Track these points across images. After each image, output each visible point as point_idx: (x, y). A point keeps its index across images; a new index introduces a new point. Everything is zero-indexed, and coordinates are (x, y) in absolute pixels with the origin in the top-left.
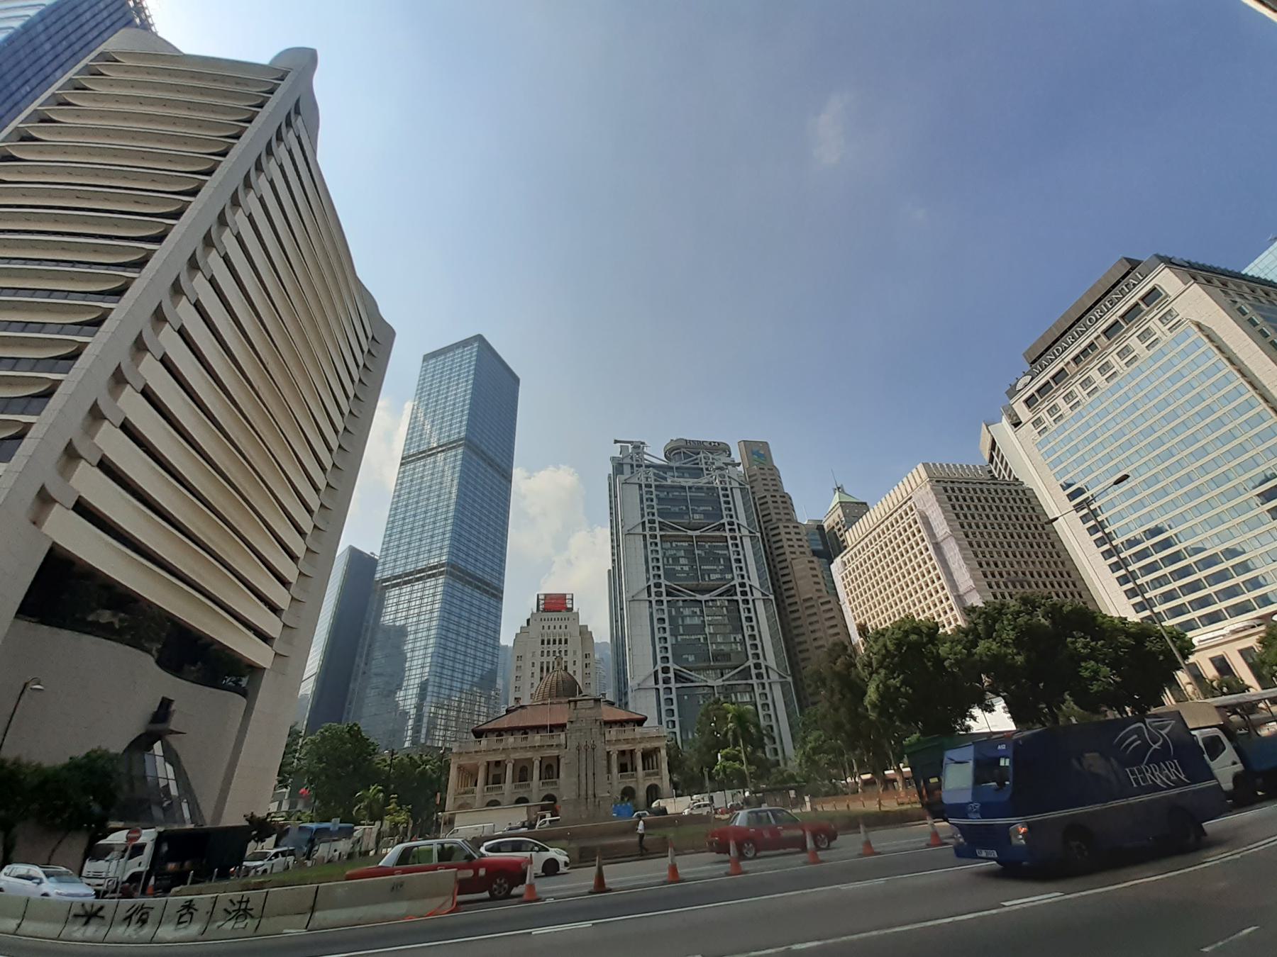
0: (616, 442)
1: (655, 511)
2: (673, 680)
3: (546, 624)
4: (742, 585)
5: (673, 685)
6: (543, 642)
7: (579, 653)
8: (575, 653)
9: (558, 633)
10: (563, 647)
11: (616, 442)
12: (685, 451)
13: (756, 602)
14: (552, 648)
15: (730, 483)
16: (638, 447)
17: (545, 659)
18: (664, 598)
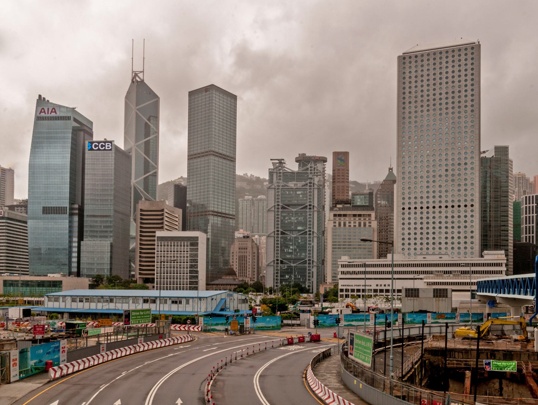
0: (271, 160)
1: (280, 200)
2: (279, 263)
3: (240, 243)
4: (310, 231)
5: (279, 265)
6: (239, 249)
7: (251, 252)
8: (249, 252)
9: (244, 246)
10: (246, 250)
11: (271, 160)
12: (303, 161)
13: (314, 238)
14: (242, 250)
15: (314, 186)
16: (281, 162)
17: (240, 254)
18: (280, 236)
